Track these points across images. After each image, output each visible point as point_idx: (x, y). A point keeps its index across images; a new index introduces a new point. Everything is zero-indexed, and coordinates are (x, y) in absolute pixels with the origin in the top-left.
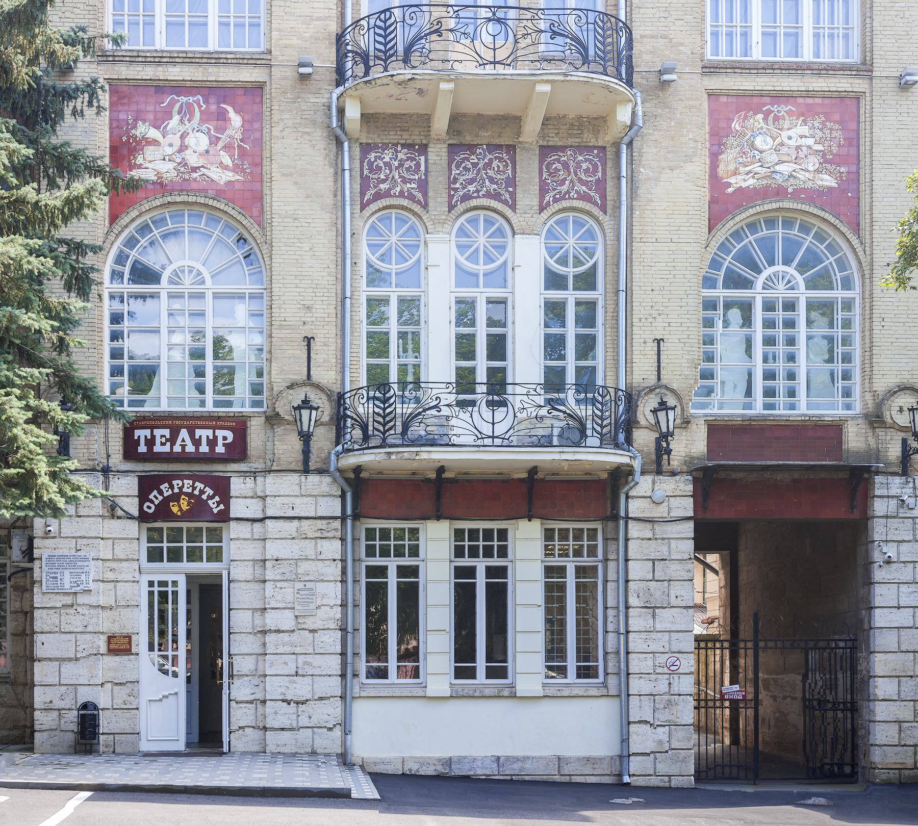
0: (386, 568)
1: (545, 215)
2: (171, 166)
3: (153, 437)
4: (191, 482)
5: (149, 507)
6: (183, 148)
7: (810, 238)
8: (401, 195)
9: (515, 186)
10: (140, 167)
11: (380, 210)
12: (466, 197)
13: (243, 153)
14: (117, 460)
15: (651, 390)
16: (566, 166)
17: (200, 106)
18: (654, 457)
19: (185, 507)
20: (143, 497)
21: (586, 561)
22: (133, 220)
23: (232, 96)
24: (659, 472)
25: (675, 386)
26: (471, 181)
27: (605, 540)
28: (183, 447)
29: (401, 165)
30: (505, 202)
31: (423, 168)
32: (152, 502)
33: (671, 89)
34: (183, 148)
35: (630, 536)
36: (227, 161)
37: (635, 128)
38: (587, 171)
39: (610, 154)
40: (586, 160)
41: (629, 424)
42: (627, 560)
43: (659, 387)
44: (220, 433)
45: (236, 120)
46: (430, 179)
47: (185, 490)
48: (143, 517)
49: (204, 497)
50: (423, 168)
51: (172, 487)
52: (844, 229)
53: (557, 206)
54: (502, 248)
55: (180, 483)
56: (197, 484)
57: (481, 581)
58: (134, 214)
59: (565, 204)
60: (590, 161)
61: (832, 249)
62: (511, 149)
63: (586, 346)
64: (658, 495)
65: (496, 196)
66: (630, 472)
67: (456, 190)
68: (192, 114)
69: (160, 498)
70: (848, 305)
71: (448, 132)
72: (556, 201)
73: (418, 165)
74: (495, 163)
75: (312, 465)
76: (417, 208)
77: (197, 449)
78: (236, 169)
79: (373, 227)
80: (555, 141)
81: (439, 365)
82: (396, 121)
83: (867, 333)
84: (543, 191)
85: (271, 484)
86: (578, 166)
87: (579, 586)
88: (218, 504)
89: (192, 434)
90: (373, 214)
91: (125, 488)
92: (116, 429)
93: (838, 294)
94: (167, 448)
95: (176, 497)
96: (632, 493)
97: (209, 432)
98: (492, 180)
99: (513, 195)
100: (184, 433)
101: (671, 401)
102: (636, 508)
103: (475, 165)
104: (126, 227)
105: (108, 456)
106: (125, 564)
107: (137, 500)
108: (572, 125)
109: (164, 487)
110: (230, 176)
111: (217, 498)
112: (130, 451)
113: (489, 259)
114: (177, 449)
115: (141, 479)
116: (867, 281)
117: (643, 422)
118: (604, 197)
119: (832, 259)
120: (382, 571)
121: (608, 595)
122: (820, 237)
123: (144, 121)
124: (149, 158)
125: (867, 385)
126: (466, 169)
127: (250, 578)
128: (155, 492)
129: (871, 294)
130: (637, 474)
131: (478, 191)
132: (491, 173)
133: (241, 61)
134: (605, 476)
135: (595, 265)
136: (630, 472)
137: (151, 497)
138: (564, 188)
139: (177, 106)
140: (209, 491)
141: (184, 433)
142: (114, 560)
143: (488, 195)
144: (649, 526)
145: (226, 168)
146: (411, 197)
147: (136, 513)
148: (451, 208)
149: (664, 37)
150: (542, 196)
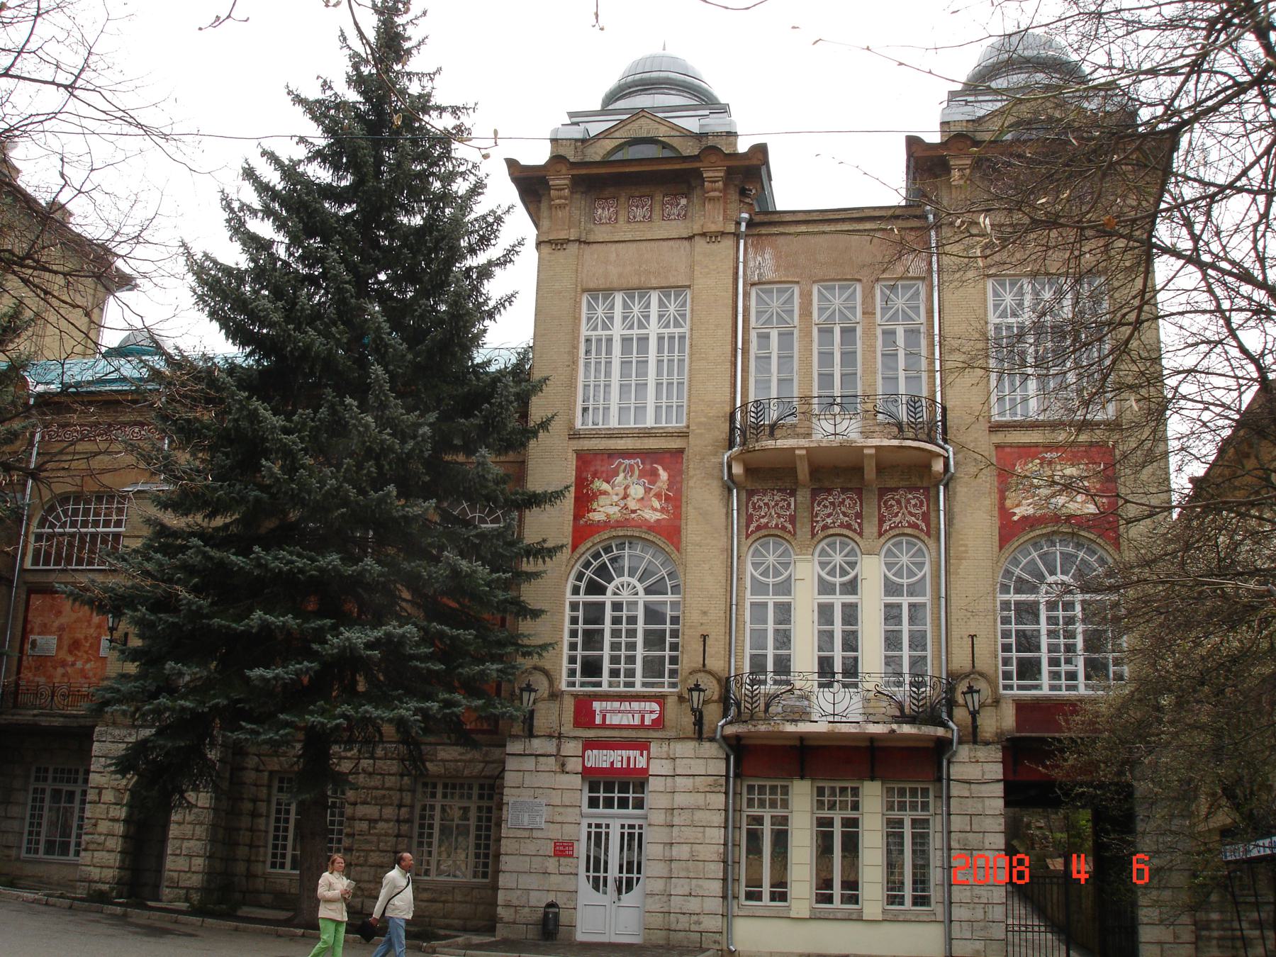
0: (762, 817)
1: (882, 540)
2: (616, 509)
6: (625, 497)
8: (777, 525)
12: (825, 527)
13: (668, 498)
14: (568, 728)
15: (967, 676)
16: (899, 502)
18: (970, 729)
21: (919, 814)
23: (661, 456)
24: (975, 742)
30: (855, 531)
34: (625, 497)
36: (657, 504)
38: (915, 506)
41: (951, 704)
45: (664, 475)
53: (892, 533)
54: (853, 565)
57: (837, 830)
59: (897, 531)
63: (917, 641)
65: (849, 527)
68: (632, 470)
72: (891, 528)
73: (789, 504)
76: (787, 536)
78: (662, 510)
79: (757, 551)
80: (891, 483)
81: (804, 658)
84: (881, 521)
86: (908, 501)
92: (569, 705)
98: (845, 514)
101: (981, 685)
102: (957, 771)
103: (832, 504)
106: (570, 810)
110: (658, 516)
113: (844, 573)
120: (759, 820)
121: (936, 841)
124: (601, 503)
126: (825, 506)
127: (662, 822)
136: (951, 741)
138: (897, 520)
144: (966, 786)
145: (655, 510)
148: (813, 535)
150: (880, 526)
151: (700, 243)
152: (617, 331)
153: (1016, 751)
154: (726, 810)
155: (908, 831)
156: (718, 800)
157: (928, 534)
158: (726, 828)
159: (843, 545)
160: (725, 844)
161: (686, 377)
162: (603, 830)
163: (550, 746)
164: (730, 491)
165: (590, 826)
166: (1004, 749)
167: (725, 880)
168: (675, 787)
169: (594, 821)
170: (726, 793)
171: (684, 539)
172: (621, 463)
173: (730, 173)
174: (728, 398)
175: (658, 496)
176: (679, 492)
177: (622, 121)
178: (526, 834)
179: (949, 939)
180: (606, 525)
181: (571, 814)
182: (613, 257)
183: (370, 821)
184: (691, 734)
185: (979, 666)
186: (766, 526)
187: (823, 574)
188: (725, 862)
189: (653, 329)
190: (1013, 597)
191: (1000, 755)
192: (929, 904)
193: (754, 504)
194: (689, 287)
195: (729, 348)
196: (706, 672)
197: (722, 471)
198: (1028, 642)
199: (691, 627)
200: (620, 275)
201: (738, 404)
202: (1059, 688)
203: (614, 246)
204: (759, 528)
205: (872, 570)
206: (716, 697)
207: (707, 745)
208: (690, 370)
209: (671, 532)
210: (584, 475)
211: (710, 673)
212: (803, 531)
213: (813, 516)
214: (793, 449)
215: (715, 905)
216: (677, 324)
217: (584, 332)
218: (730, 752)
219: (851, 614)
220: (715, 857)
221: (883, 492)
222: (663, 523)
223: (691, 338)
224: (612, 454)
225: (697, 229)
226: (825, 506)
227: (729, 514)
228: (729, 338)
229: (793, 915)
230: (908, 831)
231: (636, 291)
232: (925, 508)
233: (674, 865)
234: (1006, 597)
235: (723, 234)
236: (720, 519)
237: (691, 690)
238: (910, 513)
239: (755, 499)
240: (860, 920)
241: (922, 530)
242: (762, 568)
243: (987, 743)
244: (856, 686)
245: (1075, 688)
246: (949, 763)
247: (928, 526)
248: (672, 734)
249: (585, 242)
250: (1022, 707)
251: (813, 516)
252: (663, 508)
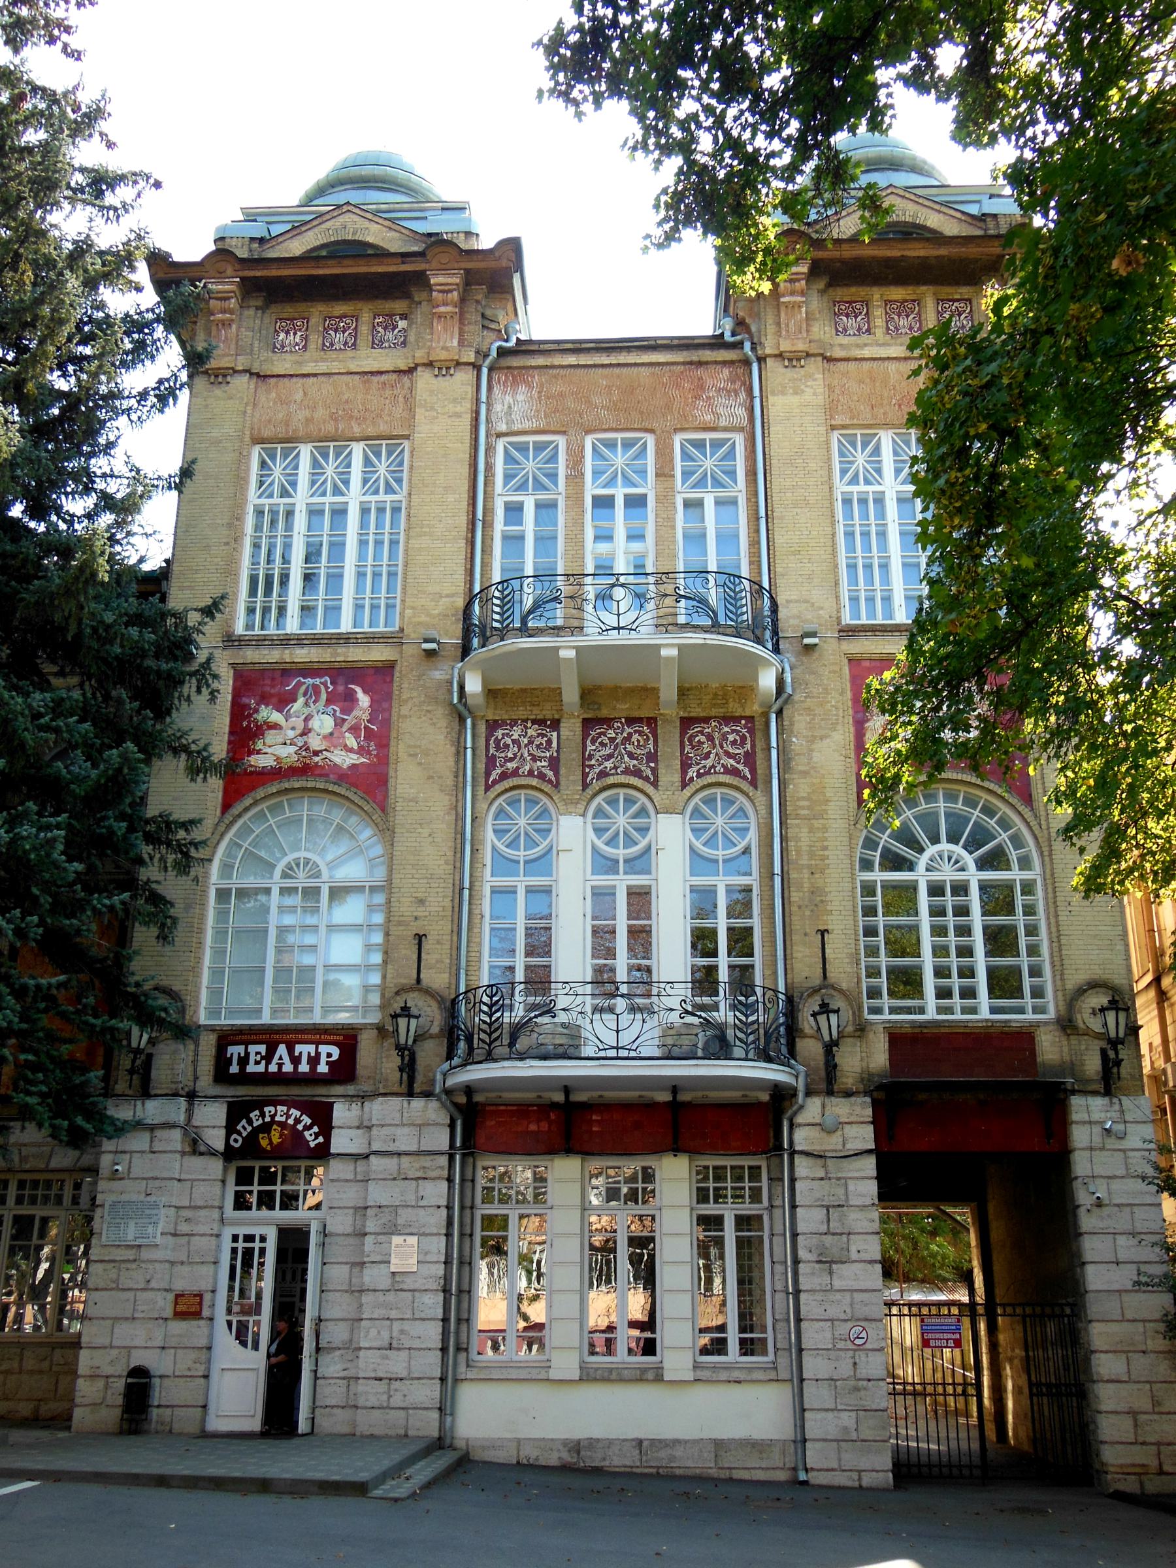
1: (687, 792)
2: (293, 749)
3: (247, 1054)
4: (285, 1109)
5: (236, 1141)
6: (306, 732)
7: (976, 813)
9: (656, 762)
10: (259, 752)
11: (506, 791)
12: (603, 774)
14: (205, 1082)
15: (816, 991)
16: (710, 738)
17: (327, 688)
18: (823, 1074)
19: (276, 1140)
20: (231, 1128)
21: (748, 1208)
22: (247, 809)
23: (363, 678)
24: (830, 1093)
25: (844, 986)
26: (609, 757)
27: (770, 1179)
28: (280, 1065)
29: (531, 742)
30: (647, 779)
31: (555, 744)
32: (240, 1134)
33: (816, 655)
34: (306, 732)
35: (797, 1175)
36: (352, 742)
37: (785, 696)
38: (734, 743)
39: (759, 724)
40: (733, 731)
41: (793, 1031)
42: (793, 1207)
43: (826, 987)
44: (324, 1049)
45: (364, 700)
46: (562, 756)
47: (277, 1118)
48: (229, 1154)
49: (300, 1127)
50: (555, 744)
51: (263, 1115)
52: (1014, 801)
55: (272, 1109)
56: (293, 1111)
58: (248, 801)
60: (737, 732)
61: (1004, 824)
62: (651, 722)
63: (741, 940)
64: (829, 1121)
65: (637, 773)
66: (793, 1093)
67: (591, 767)
69: (249, 1129)
70: (1028, 888)
71: (582, 706)
72: (699, 775)
73: (549, 742)
74: (635, 737)
76: (547, 788)
77: (296, 1068)
78: (361, 751)
80: (697, 712)
82: (526, 695)
83: (1053, 921)
84: (685, 765)
85: (378, 1109)
86: (724, 737)
87: (740, 1243)
88: (317, 1135)
89: (291, 1050)
90: (499, 795)
91: (212, 1118)
92: (208, 1044)
93: (1015, 875)
94: (261, 1068)
95: (266, 1128)
96: (799, 1119)
97: (311, 1048)
98: (631, 756)
100: (282, 1050)
102: (803, 1138)
103: (612, 740)
104: (239, 816)
105: (196, 1078)
106: (203, 1213)
107: (223, 1132)
108: (716, 694)
109: (254, 1115)
111: (315, 1129)
112: (221, 1074)
114: (273, 1068)
115: (230, 1104)
116: (1047, 859)
117: (807, 1030)
118: (753, 771)
119: (1004, 835)
121: (773, 1249)
122: (989, 811)
123: (267, 705)
125: (1059, 983)
126: (602, 744)
128: (244, 1122)
129: (1052, 874)
130: (801, 1095)
131: (616, 768)
132: (630, 748)
133: (370, 639)
134: (765, 1097)
136: (793, 1093)
137: (239, 1127)
138: (709, 763)
139: (303, 688)
140: (307, 1120)
141: (282, 1050)
142: (190, 1207)
143: (627, 771)
144: (820, 1162)
145: (351, 750)
146: (542, 776)
147: (220, 1146)
148: (585, 786)
149: (807, 601)
150: (684, 772)
151: (424, 378)
152: (302, 497)
153: (891, 1102)
154: (449, 1208)
155: (730, 1234)
156: (436, 1192)
157: (753, 783)
158: (448, 1235)
159: (629, 801)
160: (447, 1262)
161: (400, 563)
162: (257, 1245)
163: (176, 1110)
164: (462, 720)
165: (235, 1238)
166: (875, 1104)
167: (446, 1320)
168: (367, 1173)
169: (242, 1231)
170: (450, 1180)
171: (391, 792)
172: (299, 684)
173: (471, 279)
174: (460, 587)
175: (354, 730)
176: (386, 724)
177: (322, 215)
178: (130, 1254)
179: (801, 1411)
180: (277, 773)
181: (206, 1221)
182: (299, 396)
184: (396, 1089)
185: (833, 975)
186: (515, 773)
187: (600, 844)
188: (446, 1291)
189: (354, 497)
190: (878, 876)
191: (869, 1111)
192: (764, 1353)
193: (497, 741)
194: (407, 437)
195: (463, 520)
196: (420, 990)
197: (451, 692)
198: (903, 943)
199: (399, 923)
200: (309, 421)
201: (477, 589)
203: (301, 381)
204: (504, 776)
205: (671, 834)
206: (435, 1029)
207: (418, 1103)
208: (406, 550)
209: (369, 787)
210: (245, 700)
211: (428, 992)
212: (571, 778)
213: (585, 758)
214: (557, 649)
215: (431, 1363)
216: (389, 489)
217: (253, 496)
218: (457, 1115)
219: (640, 899)
221: (687, 723)
222: (362, 770)
223: (409, 507)
224: (287, 671)
225: (420, 355)
226: (602, 744)
227: (460, 753)
228: (464, 505)
229: (553, 1374)
230: (730, 1234)
231: (331, 441)
232: (748, 746)
233: (365, 1299)
234: (868, 876)
235: (458, 364)
236: (445, 762)
237: (395, 1016)
238: (728, 754)
239: (499, 733)
240: (659, 1378)
241: (745, 778)
242: (508, 837)
243: (848, 1094)
246: (791, 1126)
247: (753, 771)
248: (366, 1087)
249: (258, 375)
250: (899, 1040)
251: (585, 758)
252: (361, 748)
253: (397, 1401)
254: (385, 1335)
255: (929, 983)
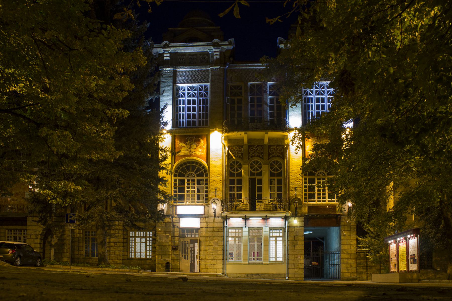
12: (252, 157)
26: (254, 153)
54: (260, 168)
65: (259, 156)
75: (216, 216)
84: (269, 155)
98: (258, 153)
99: (263, 156)
135: (282, 171)
143: (257, 156)
166: (304, 218)
183: (115, 243)
188: (223, 250)
202: (320, 201)
220: (221, 249)
238: (278, 153)
244: (261, 202)
245: (325, 201)
251: (249, 153)
253: (215, 267)
254: (212, 257)
255: (316, 196)
